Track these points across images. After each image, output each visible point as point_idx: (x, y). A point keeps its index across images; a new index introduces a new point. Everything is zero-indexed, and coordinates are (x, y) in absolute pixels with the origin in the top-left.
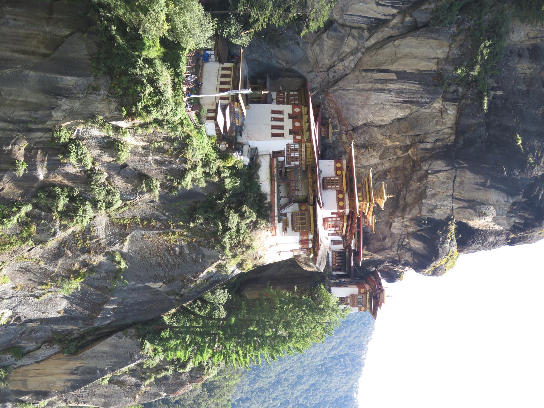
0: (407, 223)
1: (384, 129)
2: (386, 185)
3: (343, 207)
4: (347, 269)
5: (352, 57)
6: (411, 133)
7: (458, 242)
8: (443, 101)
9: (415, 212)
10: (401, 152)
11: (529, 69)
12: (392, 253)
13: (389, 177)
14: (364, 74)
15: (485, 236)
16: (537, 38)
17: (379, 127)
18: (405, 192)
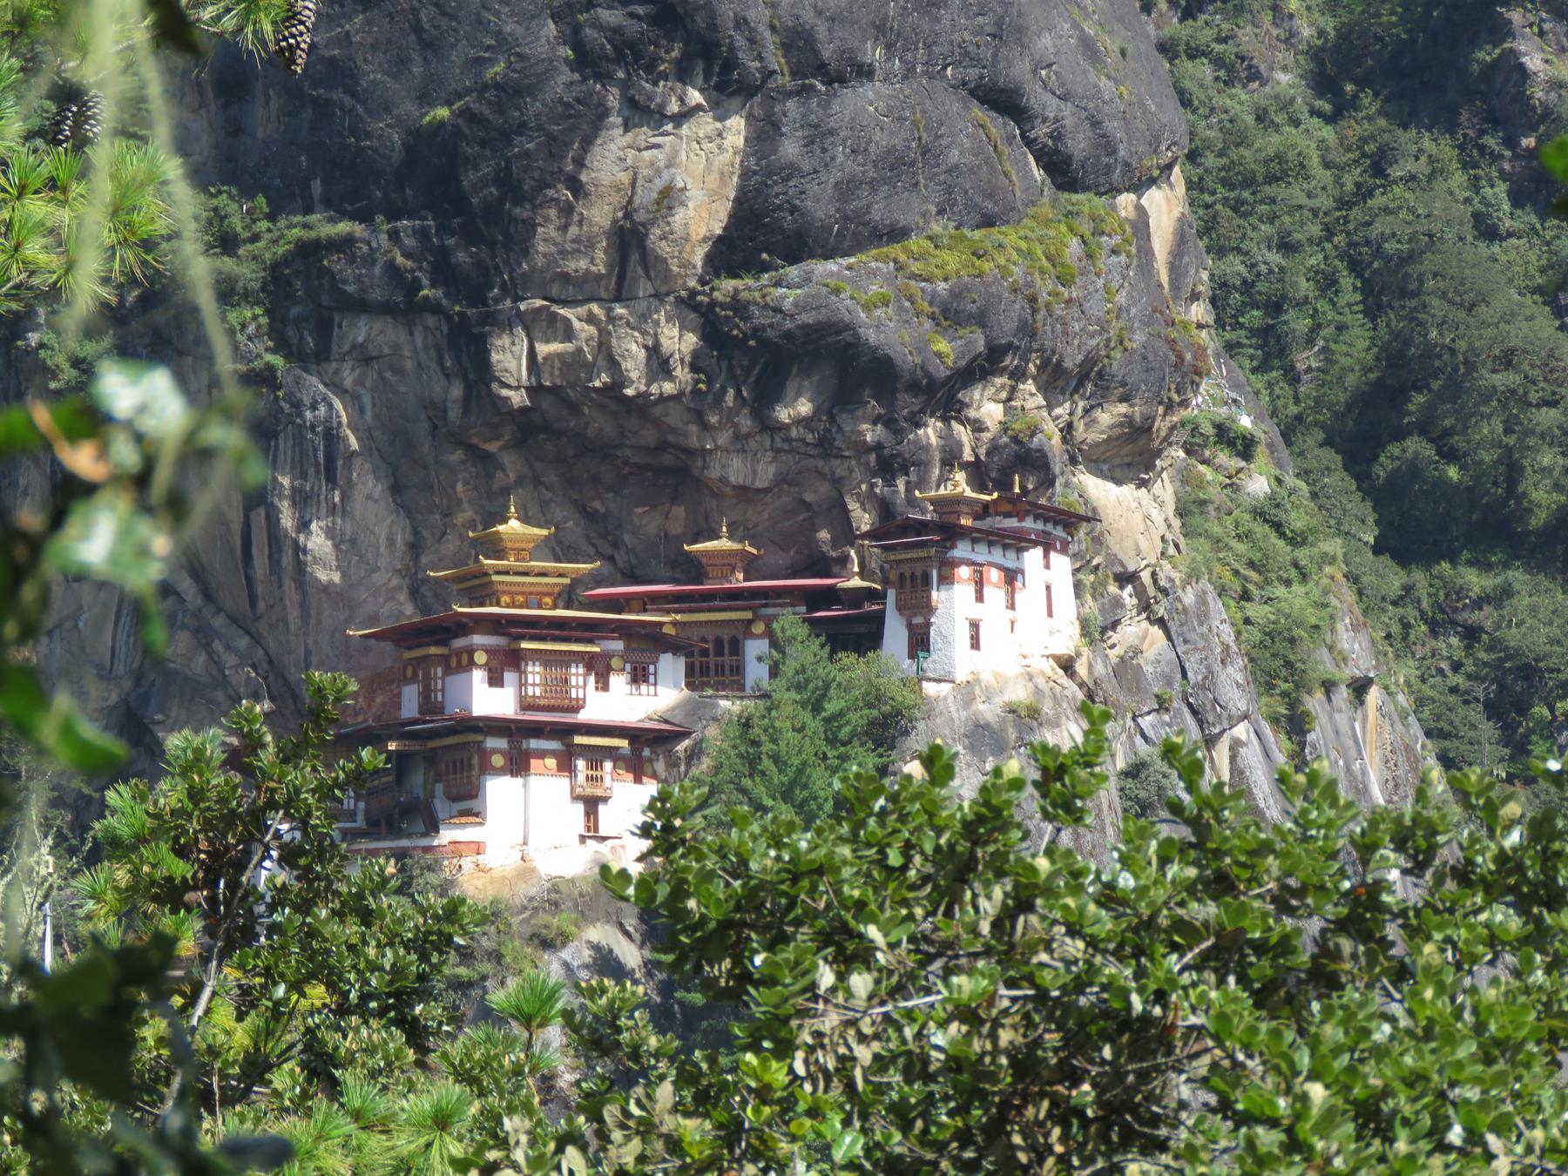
0: (724, 438)
1: (425, 533)
2: (639, 510)
3: (471, 651)
4: (862, 629)
5: (217, 645)
6: (425, 448)
7: (793, 260)
8: (327, 360)
9: (674, 416)
10: (499, 474)
11: (267, 102)
12: (857, 475)
13: (597, 505)
14: (261, 606)
15: (770, 175)
16: (199, 85)
17: (415, 548)
18: (628, 452)
